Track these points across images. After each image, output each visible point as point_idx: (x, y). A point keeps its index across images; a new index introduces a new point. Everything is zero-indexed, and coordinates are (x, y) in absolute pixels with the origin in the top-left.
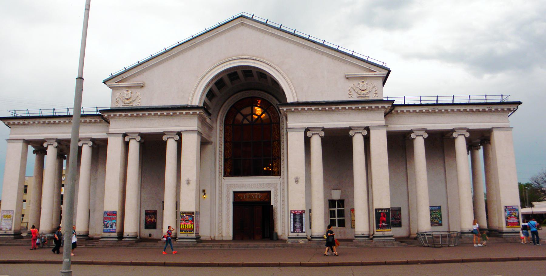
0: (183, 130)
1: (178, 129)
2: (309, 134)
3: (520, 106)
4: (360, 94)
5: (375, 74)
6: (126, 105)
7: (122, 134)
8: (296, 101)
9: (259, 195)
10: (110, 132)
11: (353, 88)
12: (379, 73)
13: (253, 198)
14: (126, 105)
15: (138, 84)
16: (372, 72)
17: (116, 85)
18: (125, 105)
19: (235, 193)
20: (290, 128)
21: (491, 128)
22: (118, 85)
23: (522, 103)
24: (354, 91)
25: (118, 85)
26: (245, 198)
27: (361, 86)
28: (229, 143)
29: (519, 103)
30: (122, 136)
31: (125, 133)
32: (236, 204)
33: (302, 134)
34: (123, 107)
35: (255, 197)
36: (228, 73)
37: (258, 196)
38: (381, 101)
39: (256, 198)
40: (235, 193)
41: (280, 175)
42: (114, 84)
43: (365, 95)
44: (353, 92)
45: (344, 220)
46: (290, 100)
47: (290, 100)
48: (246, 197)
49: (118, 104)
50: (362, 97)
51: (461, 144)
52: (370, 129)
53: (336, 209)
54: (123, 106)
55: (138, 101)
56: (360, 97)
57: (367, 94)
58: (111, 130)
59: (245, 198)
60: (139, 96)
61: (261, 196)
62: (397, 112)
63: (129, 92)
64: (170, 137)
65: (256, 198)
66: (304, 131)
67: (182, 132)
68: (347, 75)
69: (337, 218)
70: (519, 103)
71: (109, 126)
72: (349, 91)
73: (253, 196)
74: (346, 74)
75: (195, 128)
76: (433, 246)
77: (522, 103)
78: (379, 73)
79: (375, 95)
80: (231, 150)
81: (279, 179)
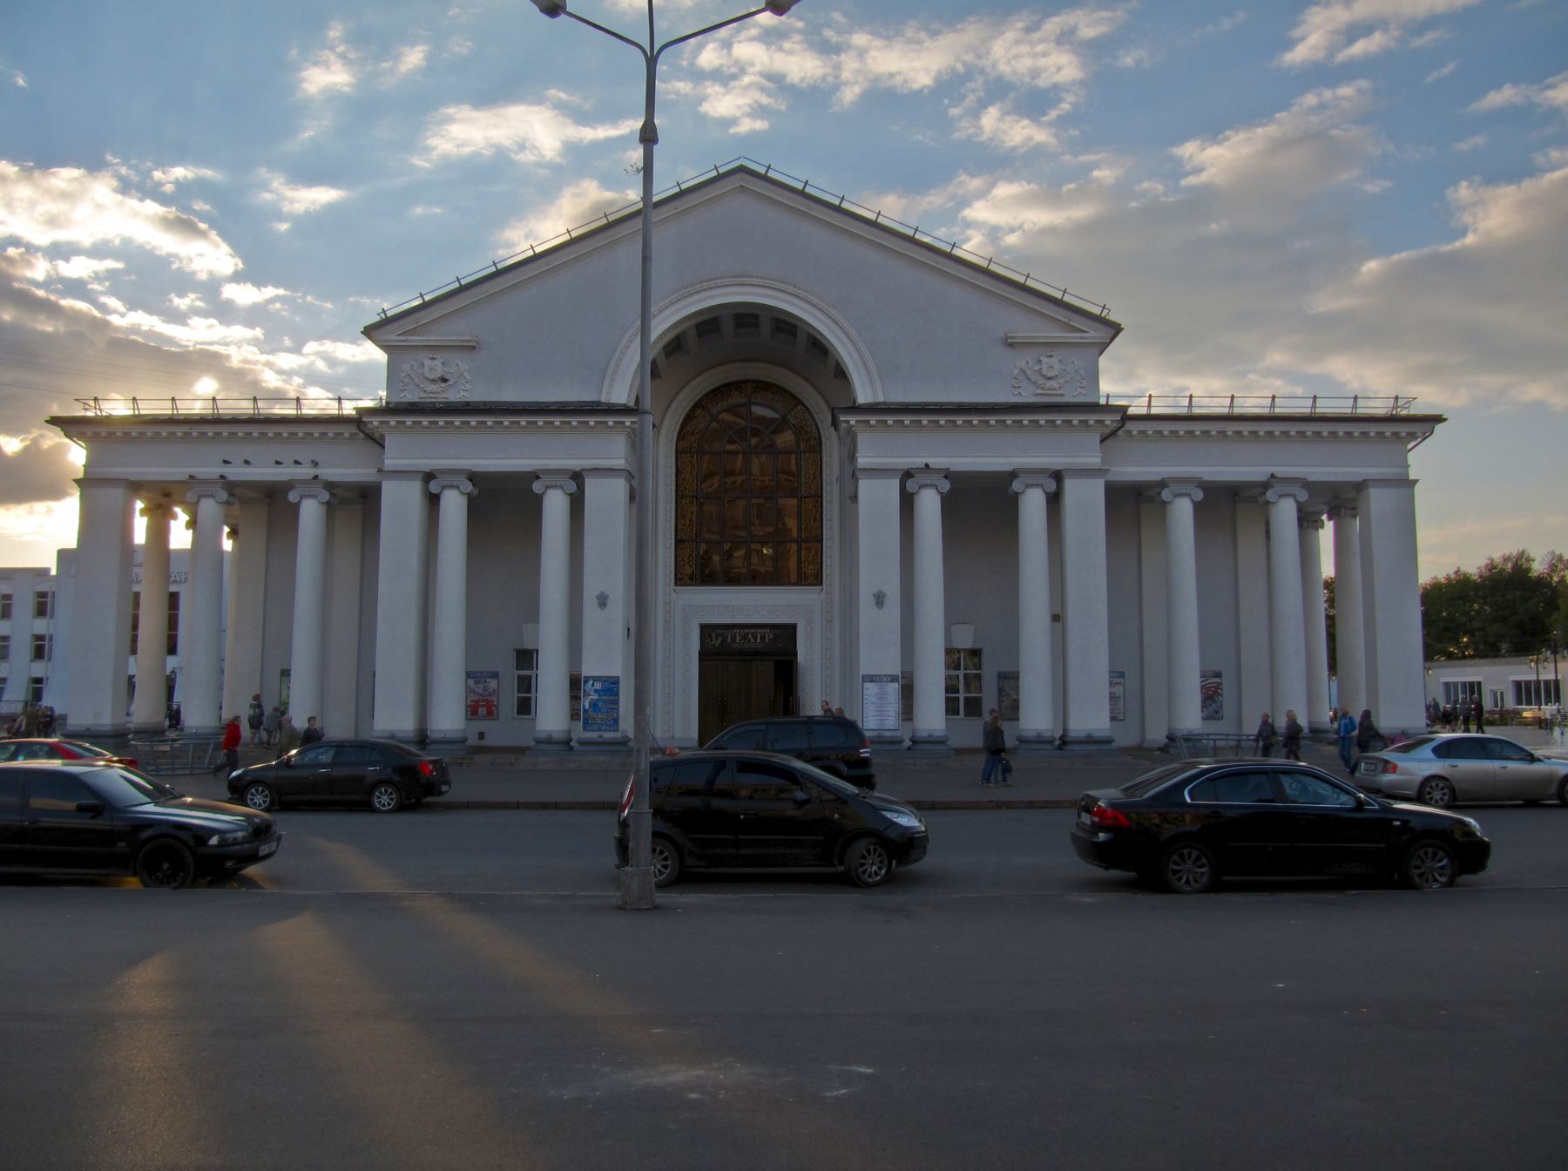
0: (588, 468)
2: (911, 485)
3: (1439, 428)
4: (1042, 388)
5: (1081, 338)
6: (430, 395)
7: (421, 475)
8: (881, 399)
9: (767, 635)
10: (386, 469)
11: (1024, 372)
12: (1092, 334)
13: (749, 642)
14: (430, 395)
15: (462, 341)
18: (425, 395)
19: (705, 628)
20: (865, 470)
21: (1365, 480)
22: (405, 341)
23: (1445, 420)
24: (1028, 378)
25: (405, 341)
26: (729, 641)
27: (1044, 367)
28: (688, 500)
29: (1438, 419)
30: (420, 478)
31: (428, 471)
32: (704, 655)
33: (895, 483)
34: (419, 400)
35: (755, 638)
36: (699, 319)
37: (763, 638)
38: (1094, 407)
39: (759, 641)
40: (705, 628)
41: (821, 584)
42: (391, 335)
43: (1055, 389)
45: (980, 698)
46: (863, 396)
47: (864, 394)
48: (734, 639)
49: (406, 393)
50: (1046, 395)
52: (1065, 476)
53: (961, 673)
54: (420, 398)
55: (463, 388)
56: (1041, 394)
57: (1060, 388)
58: (390, 462)
59: (729, 641)
60: (465, 374)
61: (771, 636)
62: (1129, 433)
63: (438, 363)
64: (554, 483)
65: (759, 641)
66: (900, 477)
67: (584, 473)
68: (1012, 338)
69: (962, 695)
70: (1438, 419)
71: (384, 453)
72: (1015, 378)
73: (750, 636)
74: (1009, 335)
75: (620, 463)
77: (1445, 420)
78: (1092, 334)
79: (1079, 390)
80: (694, 519)
81: (820, 593)
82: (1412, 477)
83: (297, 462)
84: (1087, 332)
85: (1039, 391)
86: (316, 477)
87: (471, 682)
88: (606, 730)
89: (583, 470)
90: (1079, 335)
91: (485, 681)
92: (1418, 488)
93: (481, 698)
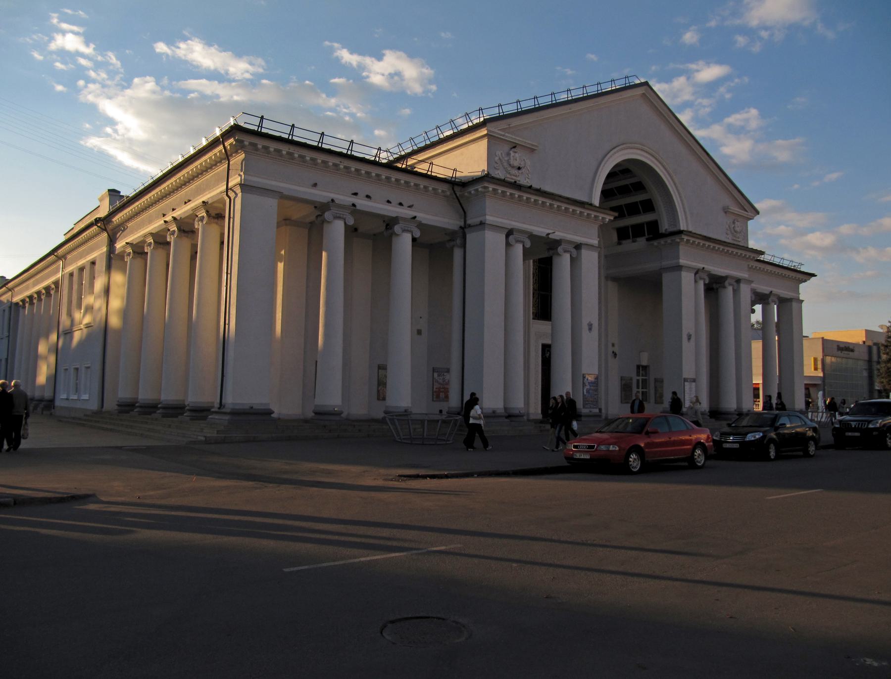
0: (584, 243)
1: (578, 239)
3: (813, 278)
12: (750, 214)
15: (533, 145)
16: (742, 210)
17: (501, 135)
22: (503, 136)
23: (816, 276)
25: (503, 136)
29: (813, 275)
44: (729, 232)
51: (404, 244)
70: (813, 275)
76: (409, 442)
77: (816, 276)
78: (750, 214)
82: (801, 298)
83: (389, 202)
84: (747, 211)
85: (735, 238)
86: (415, 217)
87: (436, 375)
88: (593, 408)
89: (580, 243)
90: (746, 213)
91: (443, 375)
92: (804, 304)
93: (442, 386)
